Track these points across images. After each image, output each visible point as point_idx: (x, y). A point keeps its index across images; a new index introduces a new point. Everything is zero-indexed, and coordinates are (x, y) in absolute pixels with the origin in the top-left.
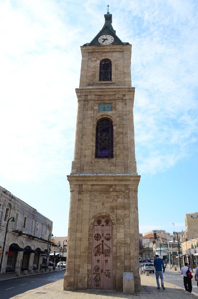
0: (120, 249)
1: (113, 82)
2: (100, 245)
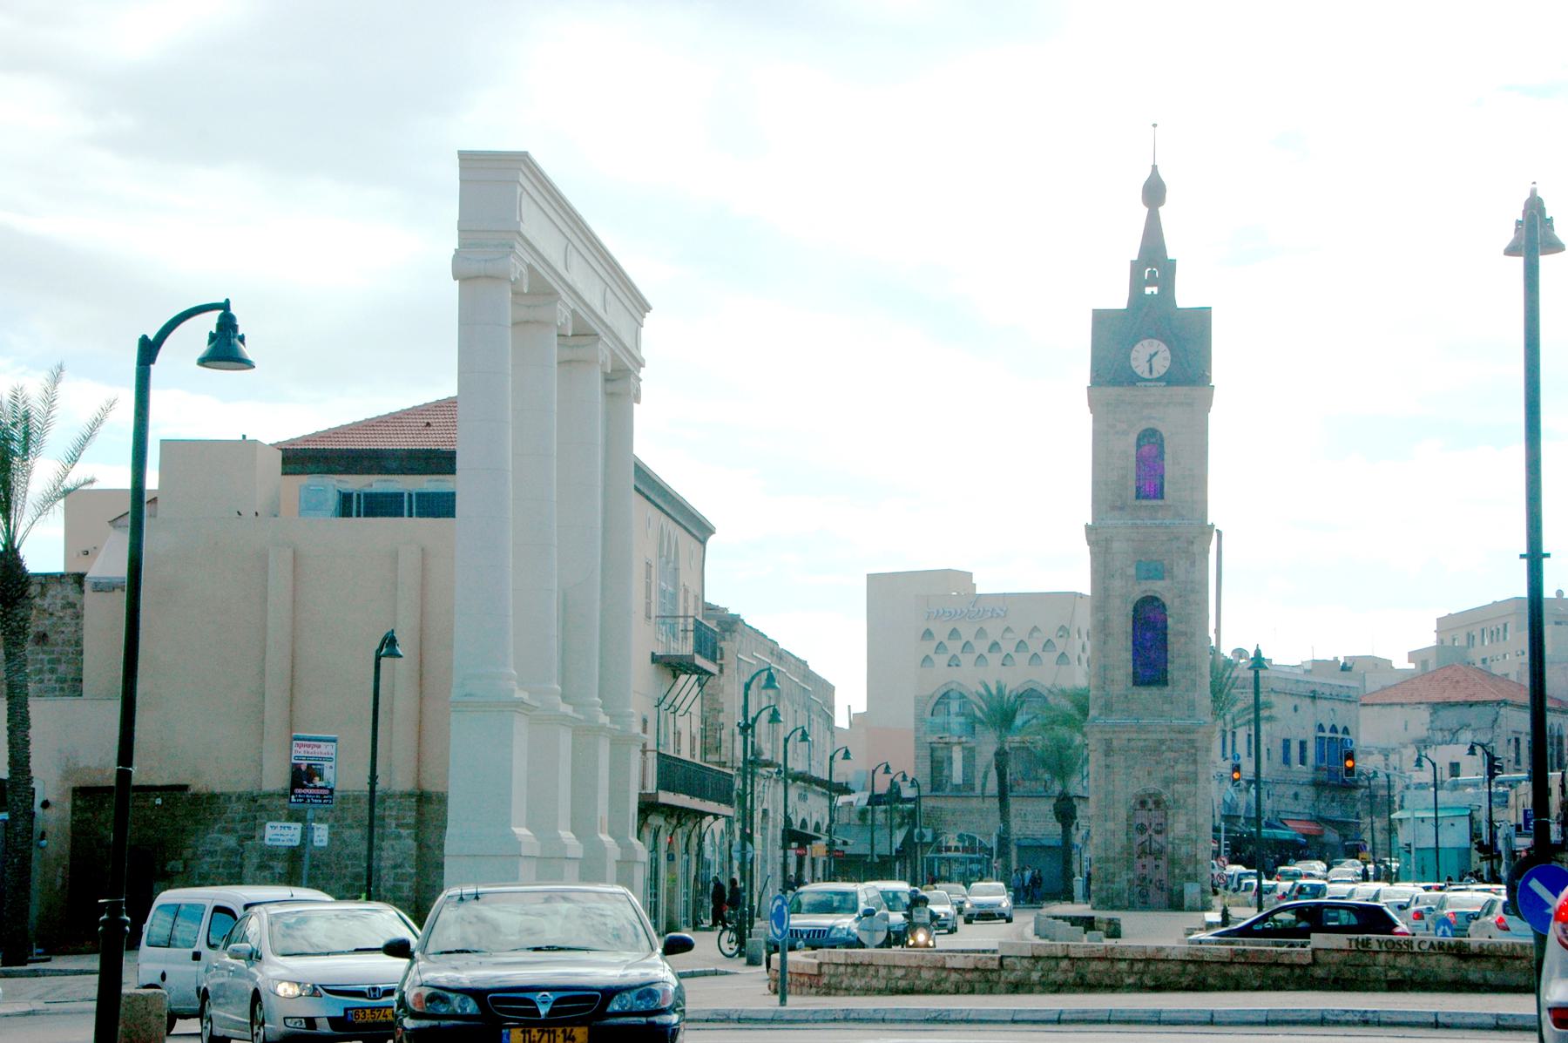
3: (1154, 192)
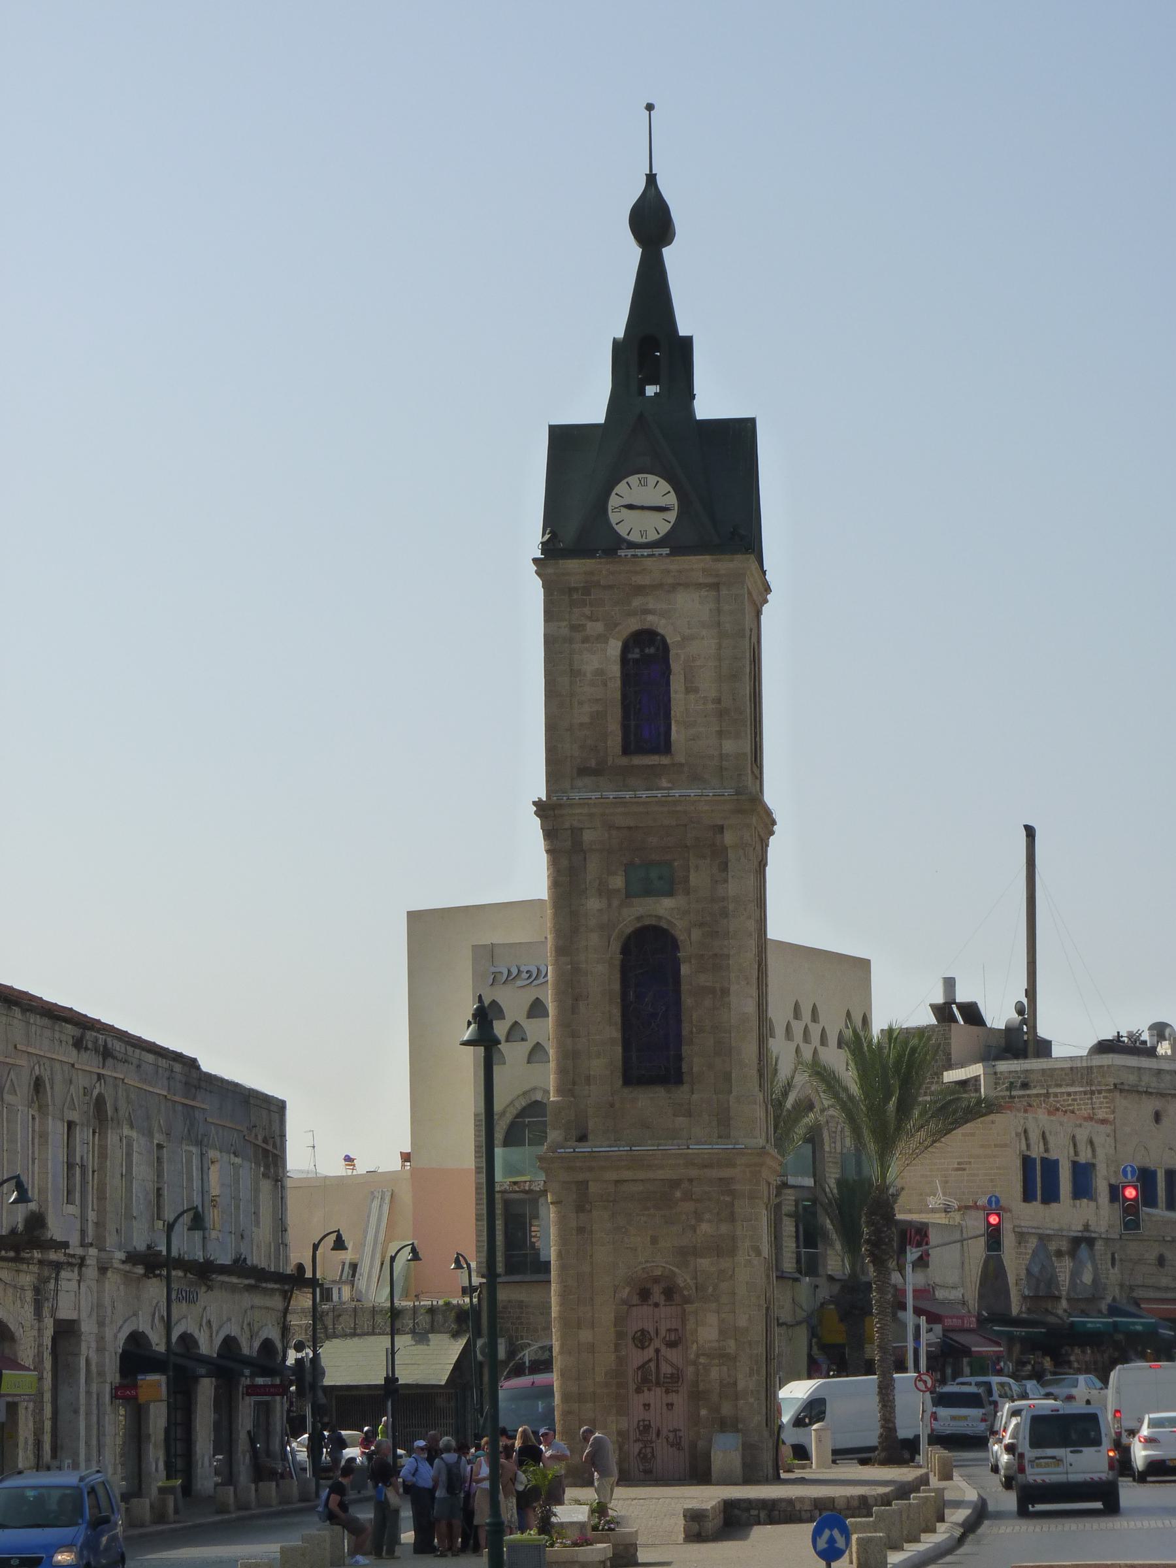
1: (680, 758)
2: (650, 1360)
3: (652, 222)
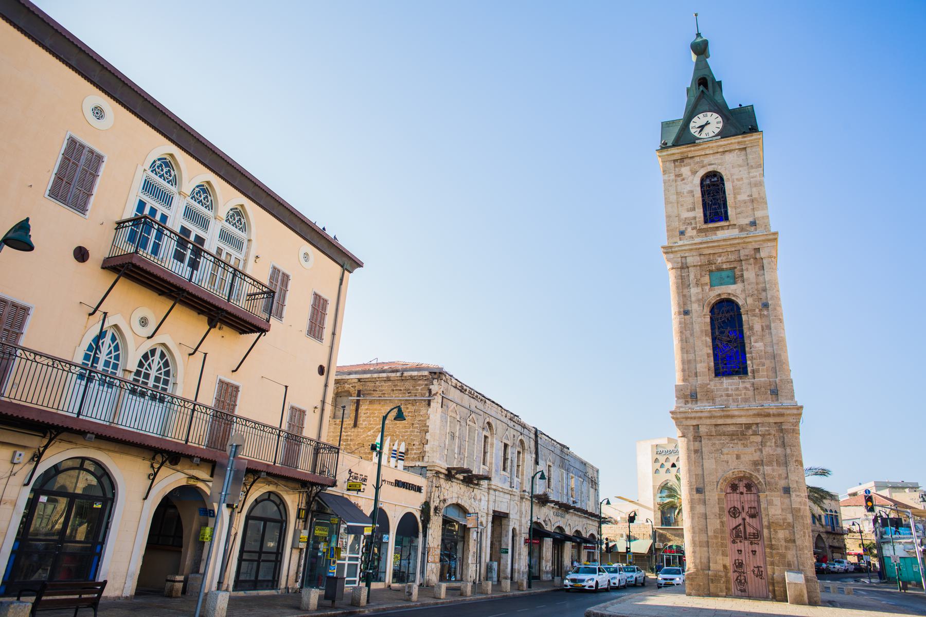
0: (776, 532)
1: (732, 223)
